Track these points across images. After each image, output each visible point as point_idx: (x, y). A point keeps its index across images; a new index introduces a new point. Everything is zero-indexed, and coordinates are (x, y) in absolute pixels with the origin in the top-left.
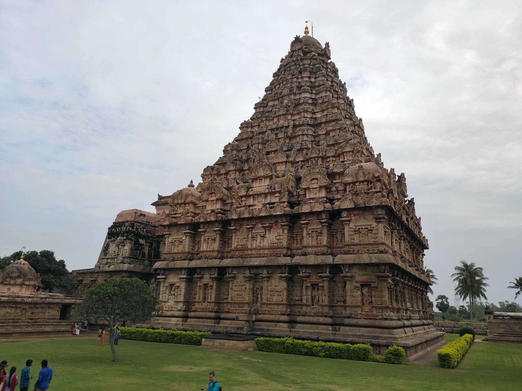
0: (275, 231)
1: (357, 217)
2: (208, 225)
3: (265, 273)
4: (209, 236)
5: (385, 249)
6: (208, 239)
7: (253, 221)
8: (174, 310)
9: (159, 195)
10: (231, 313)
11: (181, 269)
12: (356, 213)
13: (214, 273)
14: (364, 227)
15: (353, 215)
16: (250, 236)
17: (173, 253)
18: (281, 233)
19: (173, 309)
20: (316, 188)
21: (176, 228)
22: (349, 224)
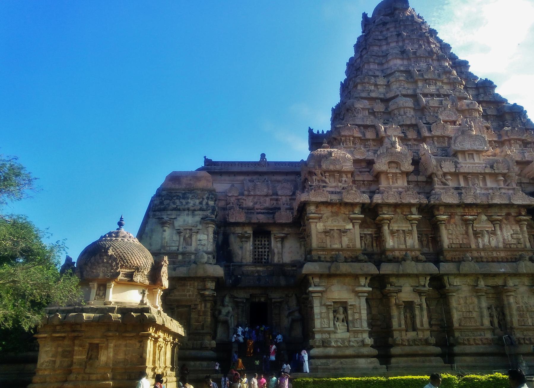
2: (393, 209)
3: (511, 283)
4: (399, 227)
6: (398, 230)
7: (473, 210)
8: (353, 346)
9: (205, 157)
10: (466, 344)
11: (356, 277)
13: (422, 283)
16: (471, 231)
17: (333, 250)
19: (352, 344)
21: (330, 209)
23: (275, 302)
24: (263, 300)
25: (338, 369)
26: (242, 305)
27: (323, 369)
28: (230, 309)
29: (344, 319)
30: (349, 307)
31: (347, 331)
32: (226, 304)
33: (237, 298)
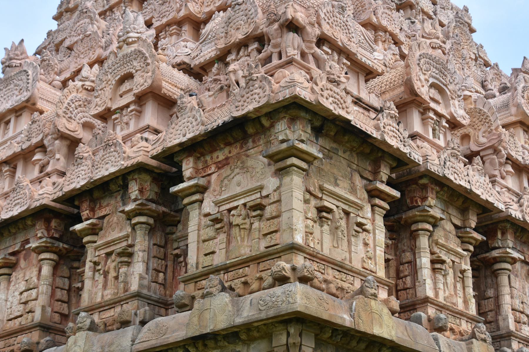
0: (22, 275)
1: (225, 171)
5: (294, 269)
12: (221, 157)
14: (242, 201)
15: (213, 169)
18: (35, 279)
20: (127, 106)
22: (201, 201)
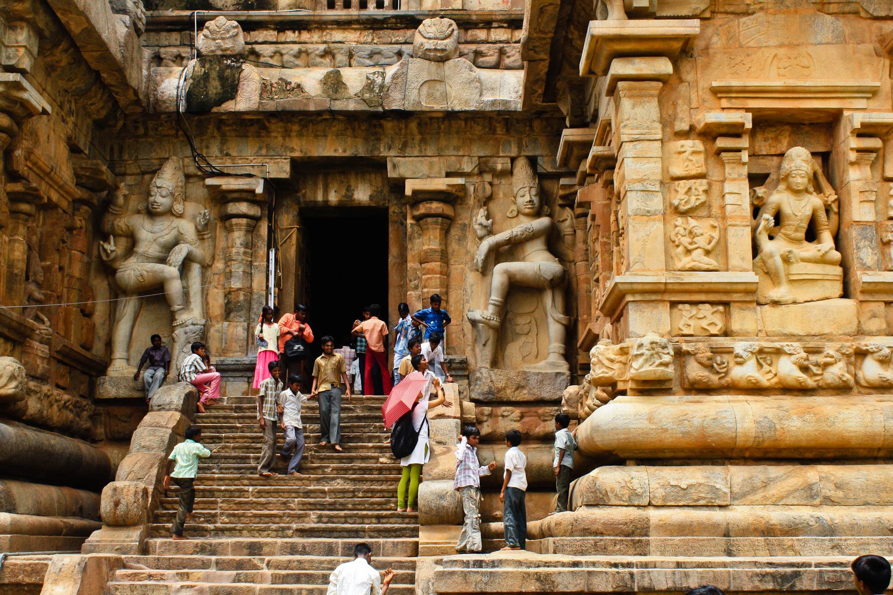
23: (421, 197)
24: (362, 194)
25: (792, 529)
26: (243, 207)
27: (682, 529)
28: (187, 227)
29: (822, 216)
30: (855, 143)
31: (838, 288)
32: (161, 200)
33: (221, 174)
